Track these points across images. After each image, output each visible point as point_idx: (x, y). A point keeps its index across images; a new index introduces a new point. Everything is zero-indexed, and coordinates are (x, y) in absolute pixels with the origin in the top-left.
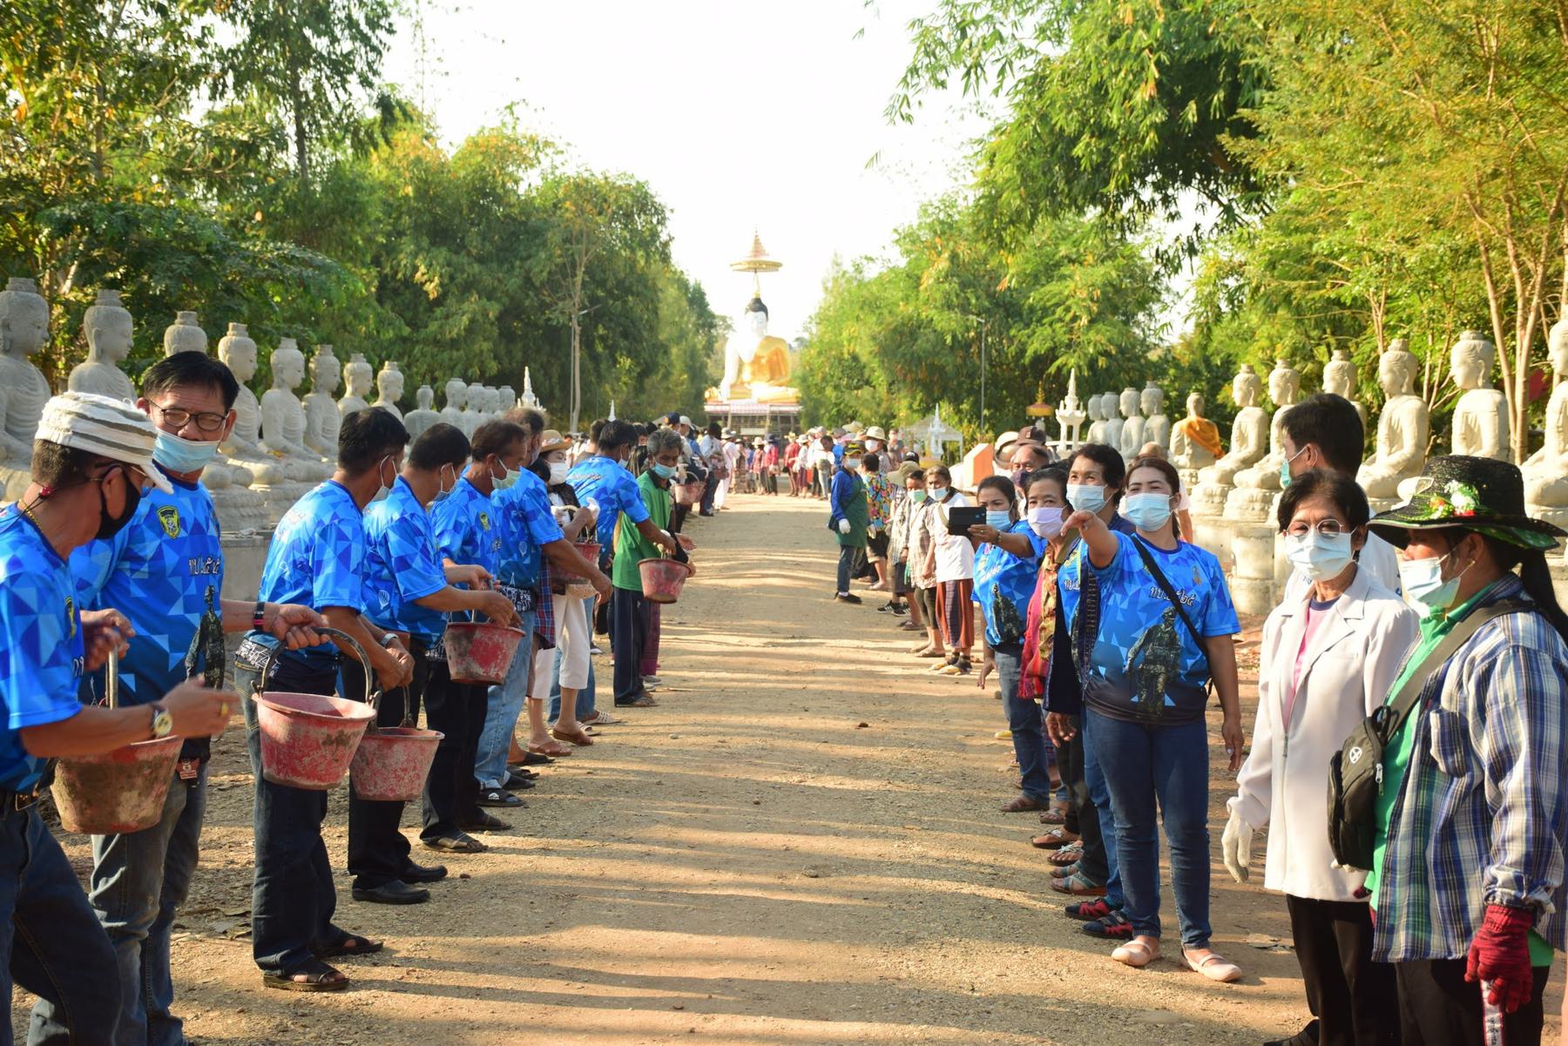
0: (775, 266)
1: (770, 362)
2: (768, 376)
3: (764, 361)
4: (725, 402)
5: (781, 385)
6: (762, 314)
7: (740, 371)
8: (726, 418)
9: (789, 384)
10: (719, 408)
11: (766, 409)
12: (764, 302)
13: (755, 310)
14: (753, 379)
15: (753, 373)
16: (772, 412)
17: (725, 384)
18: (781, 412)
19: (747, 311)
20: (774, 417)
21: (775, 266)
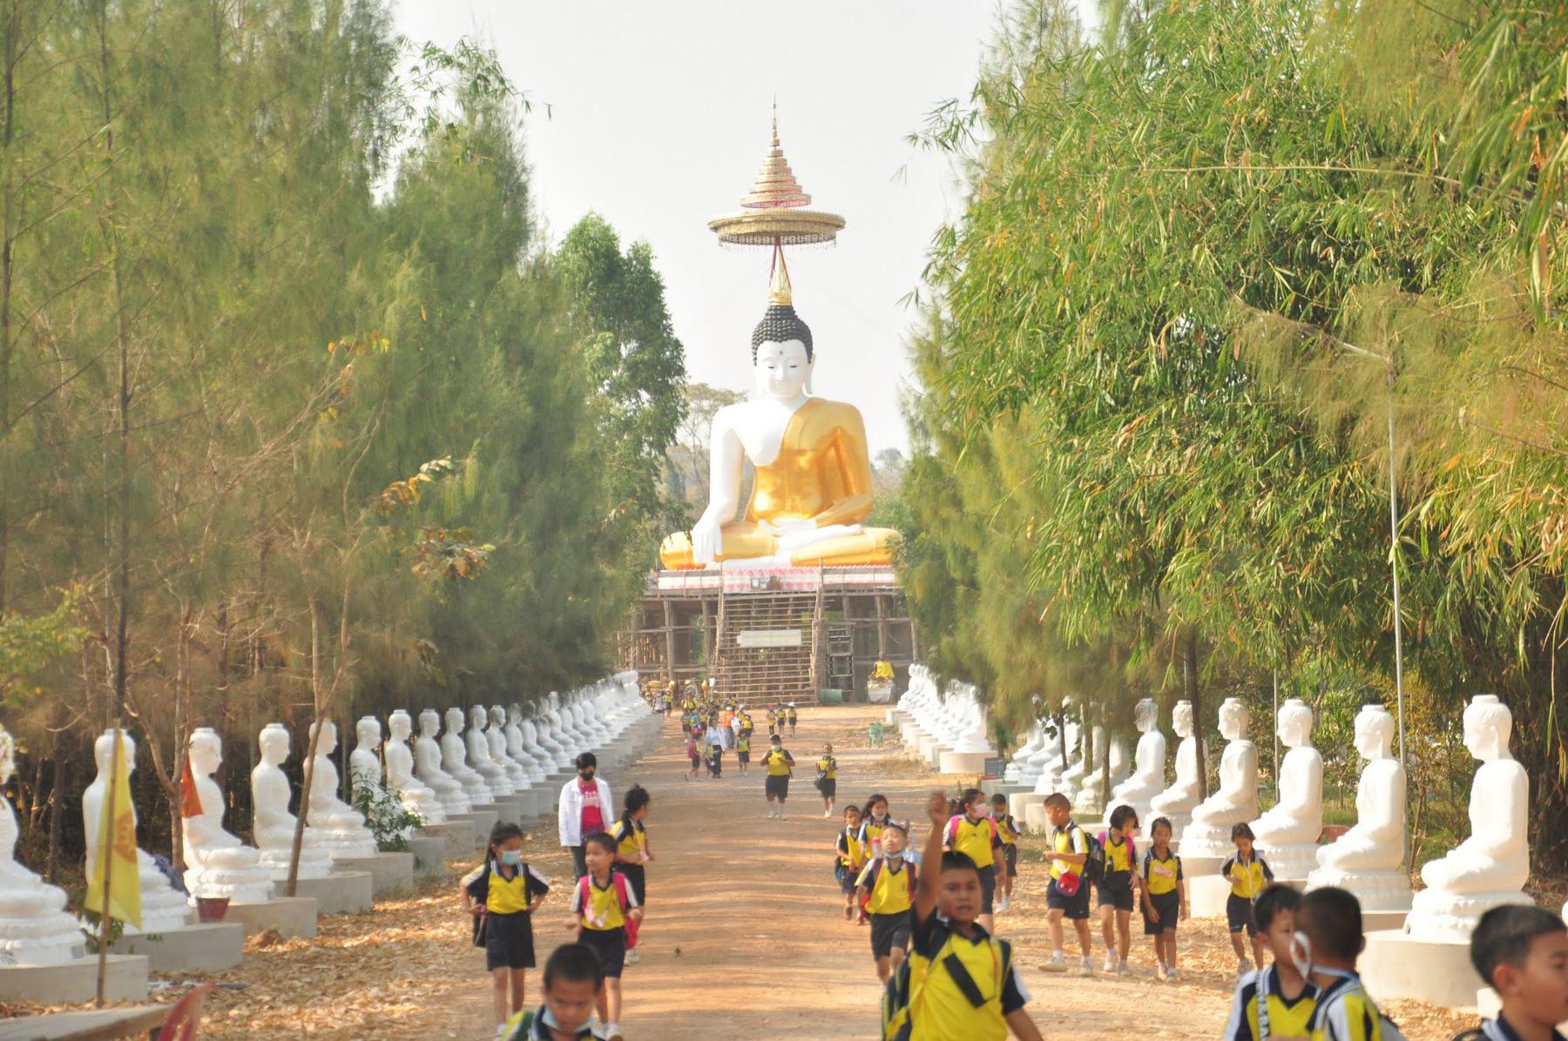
0: (825, 227)
1: (819, 462)
2: (815, 500)
3: (803, 461)
4: (711, 565)
5: (848, 521)
6: (794, 347)
7: (744, 497)
8: (713, 607)
9: (868, 519)
10: (693, 582)
11: (811, 581)
12: (801, 314)
13: (780, 336)
14: (781, 508)
15: (778, 494)
16: (828, 589)
17: (707, 526)
18: (848, 587)
19: (758, 340)
20: (834, 600)
21: (825, 227)
